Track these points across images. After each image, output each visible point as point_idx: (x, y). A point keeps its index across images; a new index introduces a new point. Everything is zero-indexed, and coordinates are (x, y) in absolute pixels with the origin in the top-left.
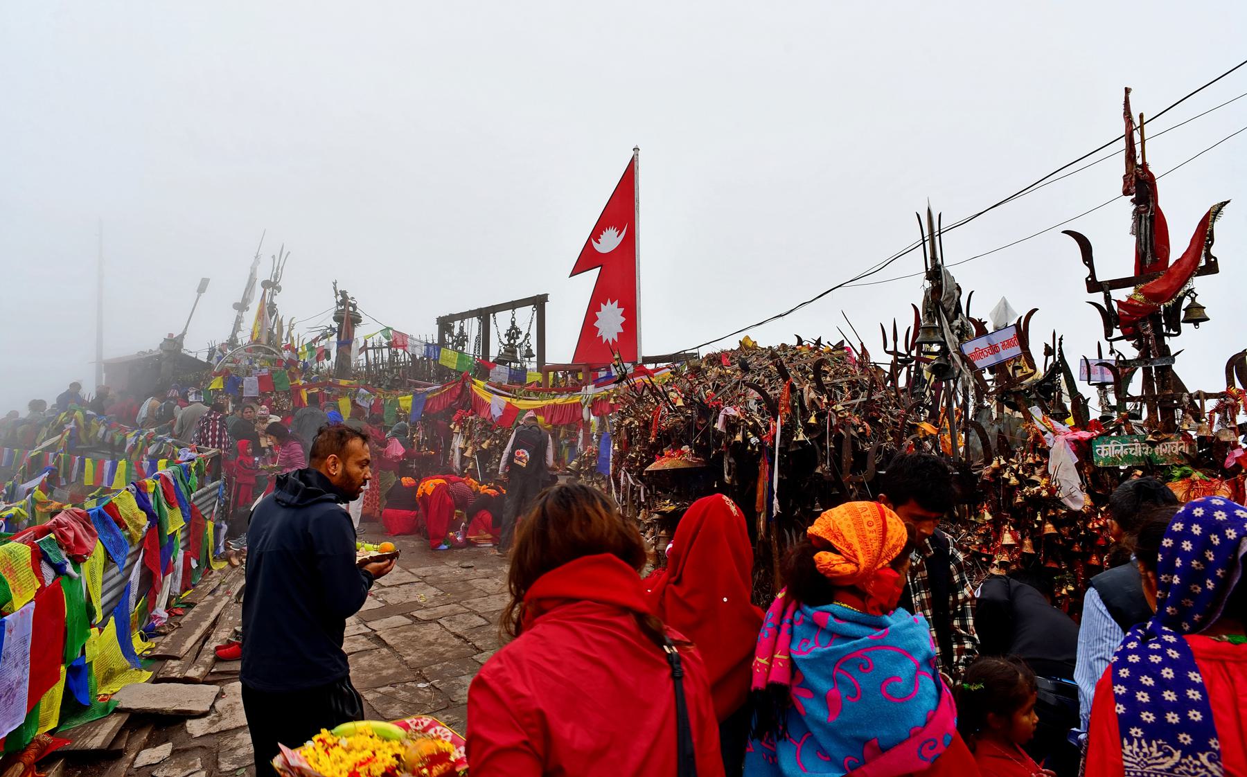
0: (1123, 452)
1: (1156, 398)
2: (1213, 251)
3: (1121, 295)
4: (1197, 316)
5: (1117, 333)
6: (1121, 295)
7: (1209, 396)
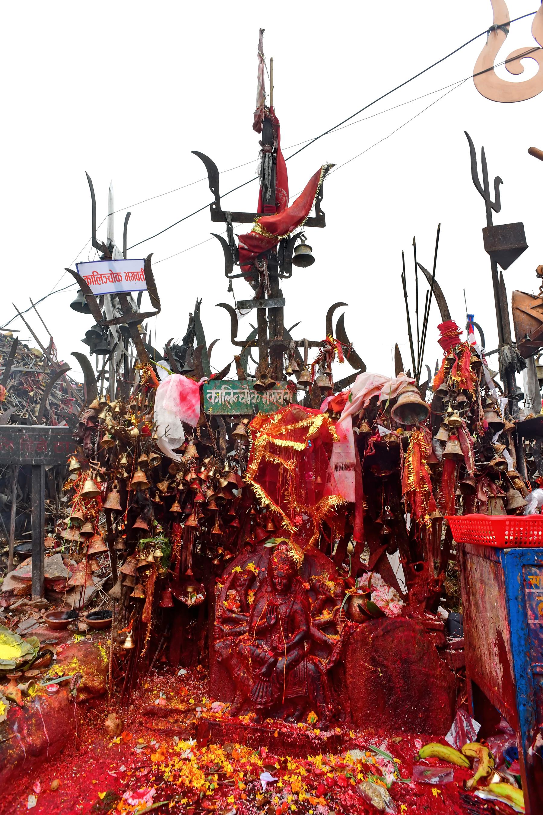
0: (232, 398)
1: (267, 343)
2: (322, 206)
3: (242, 229)
4: (306, 260)
5: (237, 269)
6: (242, 229)
7: (312, 344)
